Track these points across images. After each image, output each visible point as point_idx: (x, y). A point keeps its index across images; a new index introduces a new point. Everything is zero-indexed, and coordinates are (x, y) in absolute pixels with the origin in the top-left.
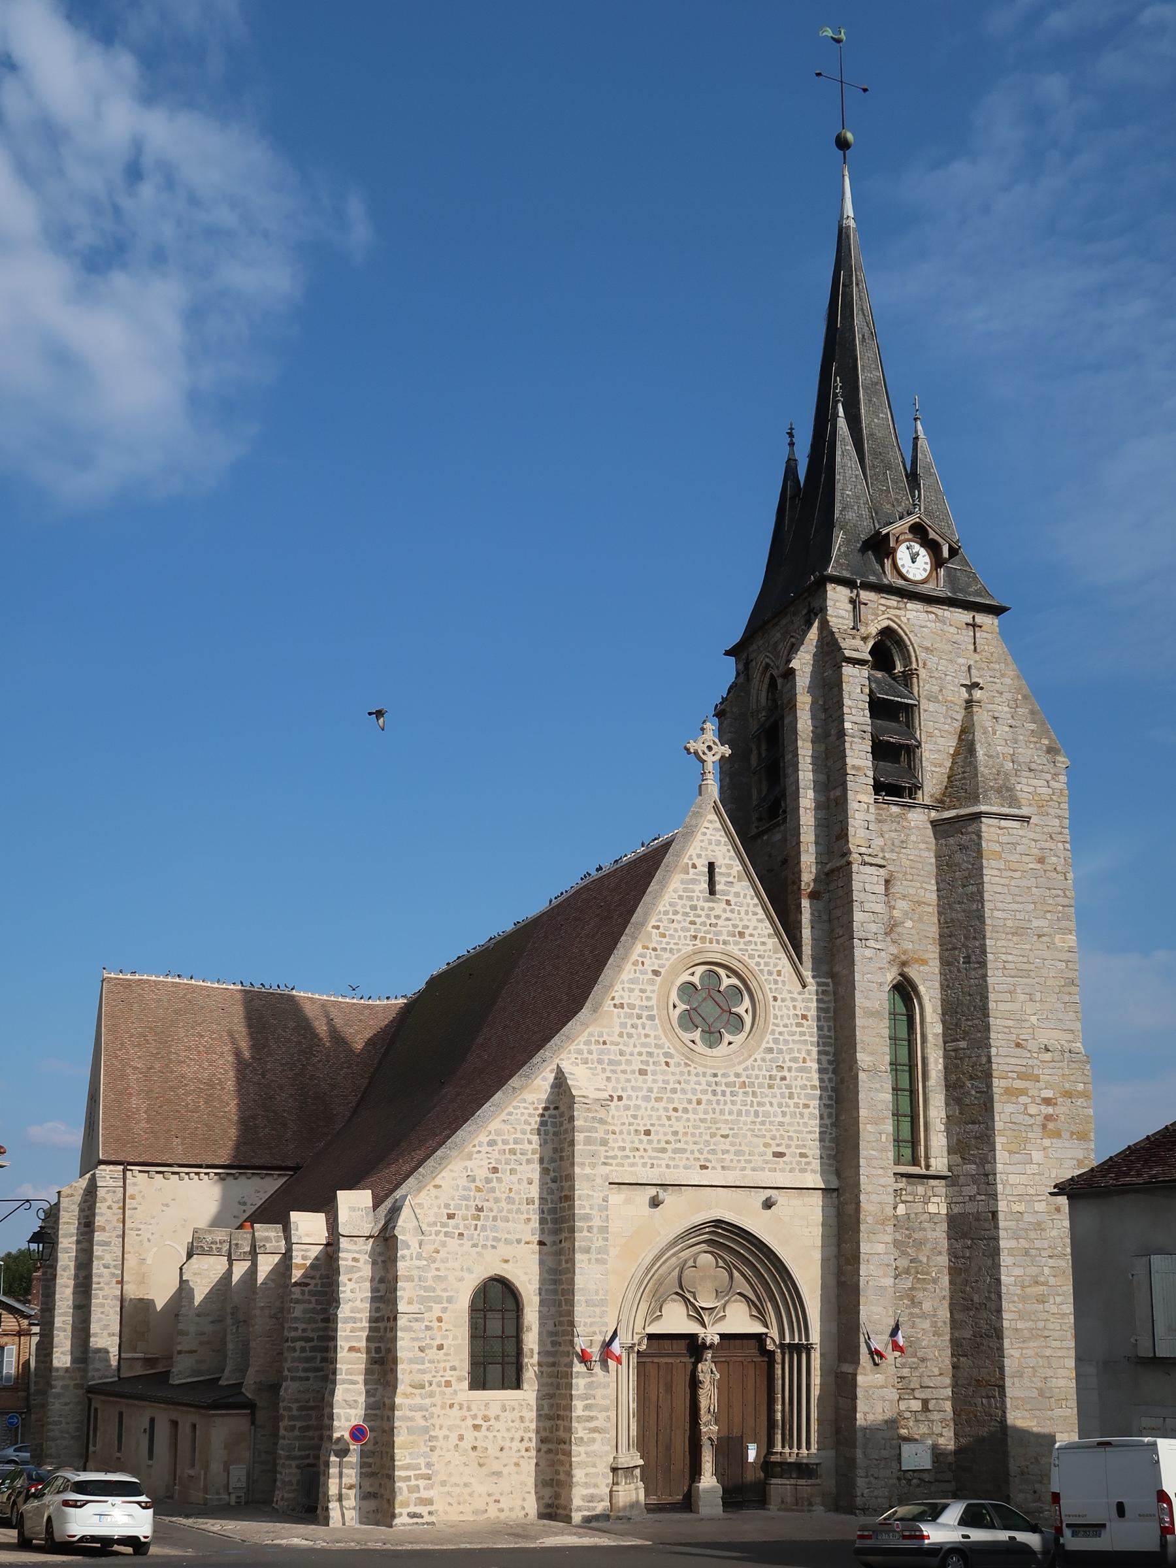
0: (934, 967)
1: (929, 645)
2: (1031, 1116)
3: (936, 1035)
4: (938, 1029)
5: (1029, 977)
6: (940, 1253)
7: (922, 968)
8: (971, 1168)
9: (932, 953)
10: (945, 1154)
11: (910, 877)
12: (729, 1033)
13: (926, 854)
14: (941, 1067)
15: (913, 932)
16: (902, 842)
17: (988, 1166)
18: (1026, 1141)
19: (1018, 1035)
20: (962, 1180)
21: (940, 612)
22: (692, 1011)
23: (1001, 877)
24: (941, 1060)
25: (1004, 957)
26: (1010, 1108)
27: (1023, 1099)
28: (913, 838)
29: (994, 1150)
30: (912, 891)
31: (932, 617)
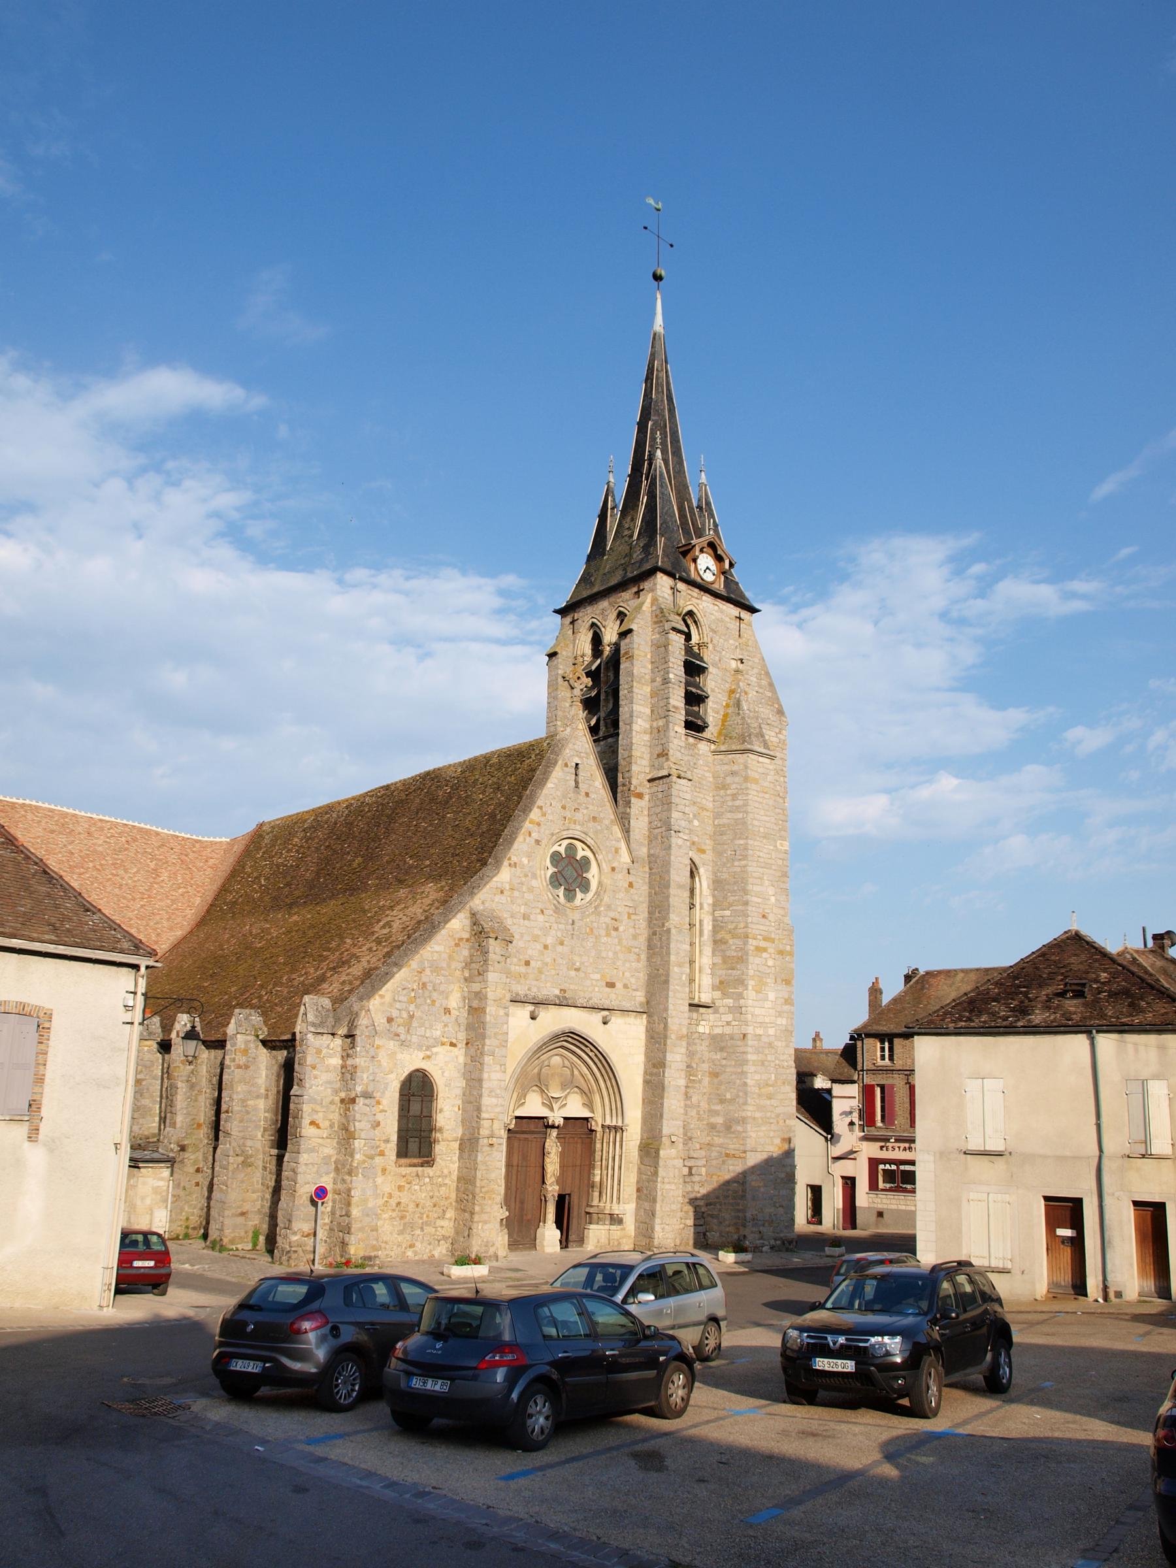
0: (709, 856)
1: (714, 628)
2: (769, 967)
3: (709, 904)
4: (710, 900)
5: (770, 868)
6: (704, 1062)
7: (702, 856)
8: (730, 1002)
9: (708, 845)
10: (710, 990)
11: (698, 790)
12: (581, 891)
13: (707, 774)
14: (710, 928)
15: (699, 829)
16: (695, 764)
17: (742, 1002)
18: (766, 984)
19: (764, 909)
20: (721, 1010)
21: (721, 605)
22: (558, 874)
23: (758, 796)
24: (711, 923)
25: (758, 853)
26: (757, 960)
27: (765, 955)
28: (701, 762)
29: (747, 989)
30: (699, 800)
31: (716, 608)
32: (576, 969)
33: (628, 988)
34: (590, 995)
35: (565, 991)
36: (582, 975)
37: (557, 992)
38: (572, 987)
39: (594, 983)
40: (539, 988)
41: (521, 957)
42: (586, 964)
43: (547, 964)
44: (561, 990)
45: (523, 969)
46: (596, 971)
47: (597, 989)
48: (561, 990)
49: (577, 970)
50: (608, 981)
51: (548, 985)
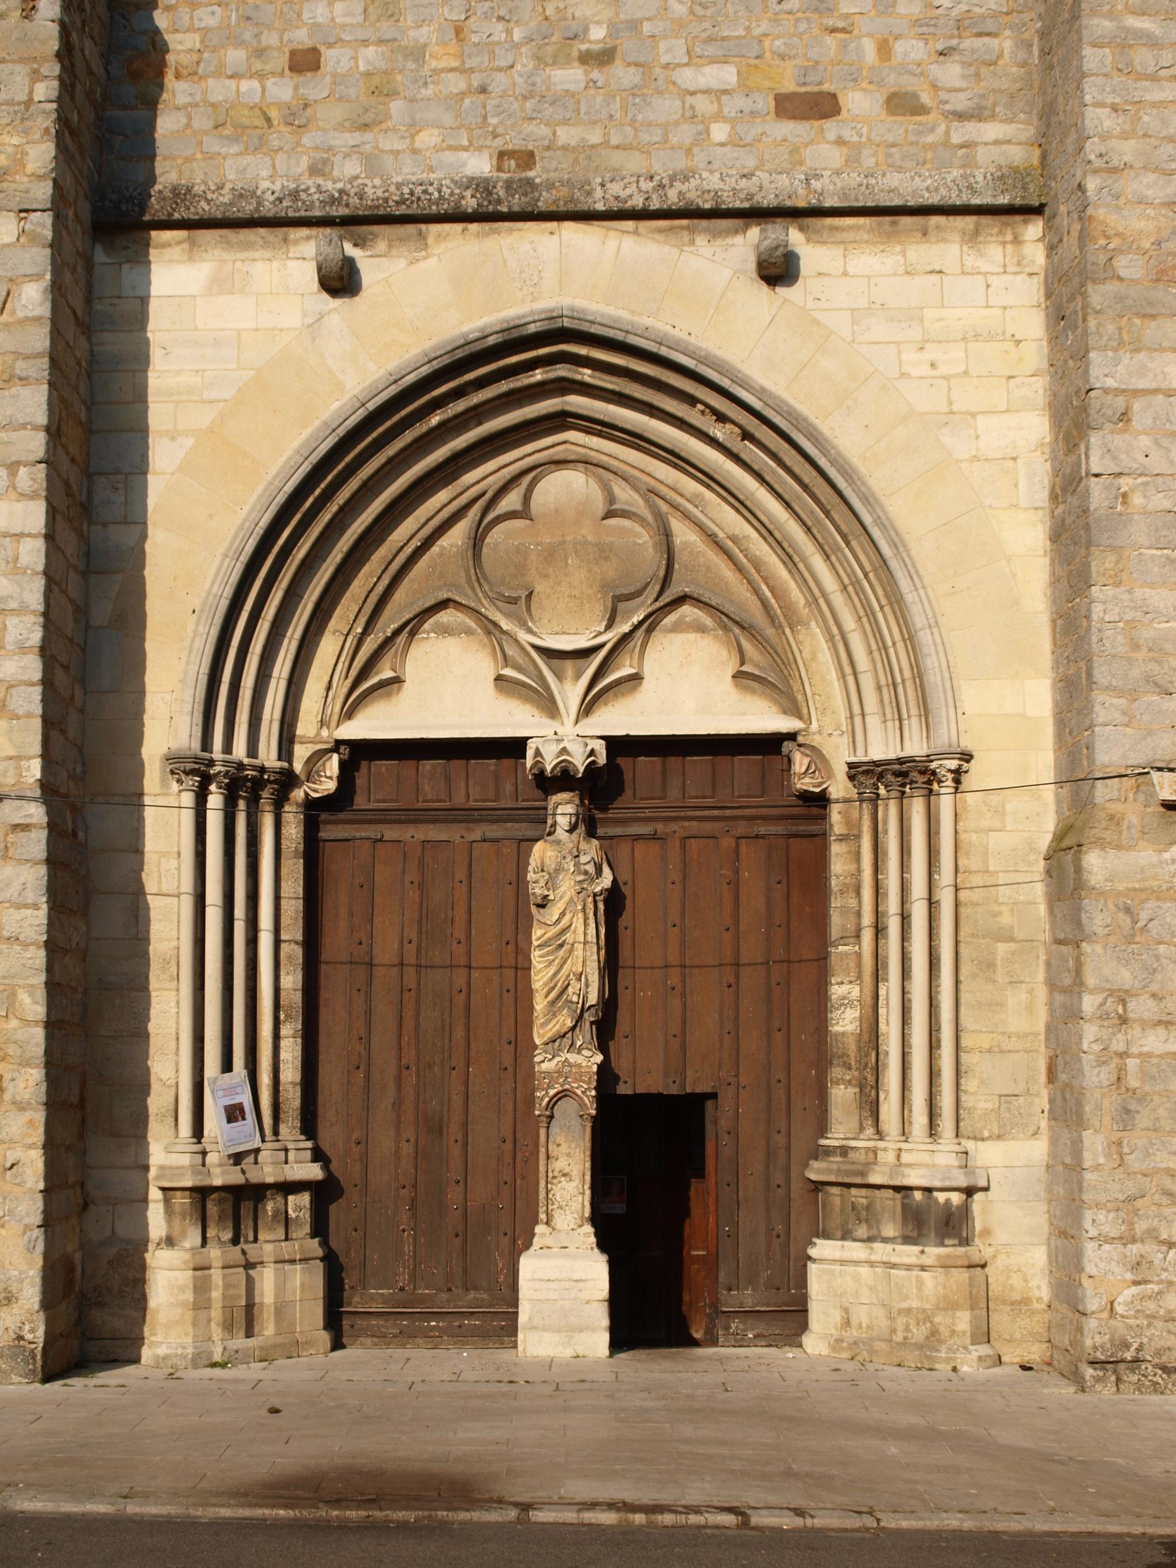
32: (586, 58)
33: (920, 110)
34: (681, 163)
35: (527, 159)
36: (622, 75)
37: (480, 165)
38: (566, 135)
39: (703, 105)
40: (371, 162)
41: (270, 39)
42: (647, 28)
43: (418, 53)
44: (502, 155)
45: (282, 90)
46: (711, 50)
47: (719, 132)
48: (502, 155)
49: (603, 57)
50: (790, 86)
51: (427, 139)
